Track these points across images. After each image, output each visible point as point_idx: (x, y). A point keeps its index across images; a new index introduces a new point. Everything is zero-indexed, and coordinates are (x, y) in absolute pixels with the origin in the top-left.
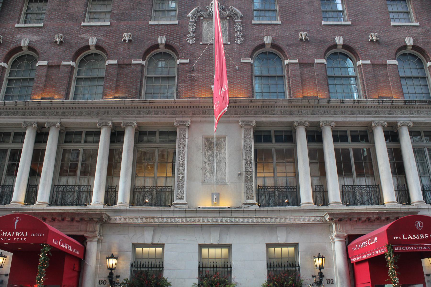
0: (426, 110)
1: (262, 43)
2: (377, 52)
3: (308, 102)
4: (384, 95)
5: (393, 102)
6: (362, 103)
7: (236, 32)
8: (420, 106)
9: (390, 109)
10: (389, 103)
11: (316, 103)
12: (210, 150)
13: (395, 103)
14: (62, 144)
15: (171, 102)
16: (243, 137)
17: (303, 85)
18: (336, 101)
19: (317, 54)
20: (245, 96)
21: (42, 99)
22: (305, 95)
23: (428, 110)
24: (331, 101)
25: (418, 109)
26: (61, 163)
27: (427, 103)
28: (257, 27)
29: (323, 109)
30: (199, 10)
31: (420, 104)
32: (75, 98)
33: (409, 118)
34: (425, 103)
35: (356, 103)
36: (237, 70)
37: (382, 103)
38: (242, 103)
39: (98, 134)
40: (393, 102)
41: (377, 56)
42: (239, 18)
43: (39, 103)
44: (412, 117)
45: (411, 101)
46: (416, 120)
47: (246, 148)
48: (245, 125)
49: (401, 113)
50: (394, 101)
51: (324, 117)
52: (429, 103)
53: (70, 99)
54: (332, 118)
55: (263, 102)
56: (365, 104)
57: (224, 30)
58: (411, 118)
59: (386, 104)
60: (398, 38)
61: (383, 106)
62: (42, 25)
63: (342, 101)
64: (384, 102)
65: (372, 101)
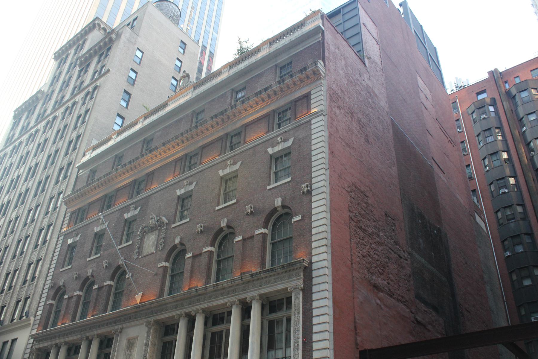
0: (274, 277)
1: (174, 244)
2: (249, 225)
3: (184, 295)
4: (246, 270)
5: (242, 279)
6: (220, 286)
7: (161, 239)
8: (263, 276)
9: (244, 285)
10: (239, 280)
11: (189, 294)
12: (129, 350)
13: (244, 278)
14: (210, 328)
15: (107, 315)
16: (146, 335)
17: (191, 277)
18: (202, 289)
19: (206, 243)
20: (155, 298)
21: (62, 324)
22: (191, 287)
23: (276, 277)
24: (198, 290)
25: (266, 279)
26: (211, 348)
27: (270, 271)
28: (174, 229)
29: (197, 298)
30: (144, 227)
31: (264, 274)
32: (217, 280)
33: (257, 291)
34: (268, 272)
35: (215, 287)
36: (155, 275)
37: (234, 281)
38: (146, 306)
39: (229, 314)
40: (242, 279)
41: (249, 229)
42: (165, 225)
43: (60, 328)
44: (260, 289)
45: (256, 273)
46: (263, 291)
47: (146, 345)
48: (148, 324)
49: (253, 287)
50: (243, 278)
51: (195, 305)
52: (271, 271)
53: (212, 283)
54: (201, 305)
55: (158, 302)
56: (222, 286)
57: (155, 241)
58: (259, 291)
59: (237, 281)
60: (270, 203)
61: (234, 284)
62: (188, 220)
63: (205, 288)
64: (235, 280)
65: (227, 282)
